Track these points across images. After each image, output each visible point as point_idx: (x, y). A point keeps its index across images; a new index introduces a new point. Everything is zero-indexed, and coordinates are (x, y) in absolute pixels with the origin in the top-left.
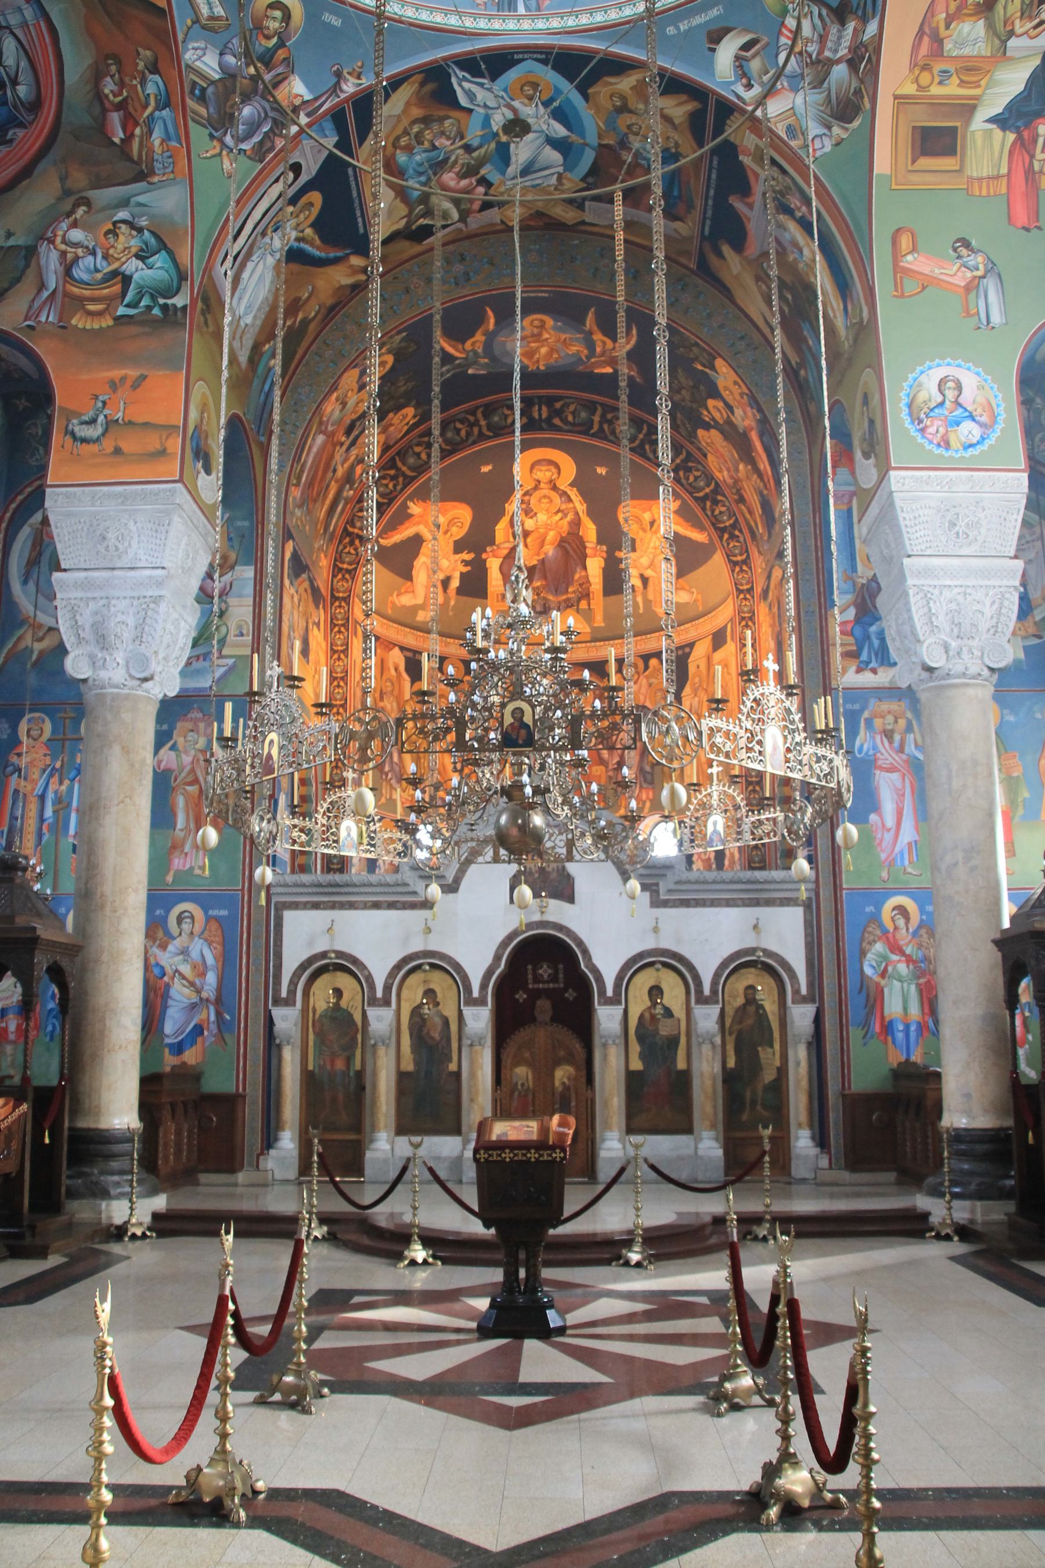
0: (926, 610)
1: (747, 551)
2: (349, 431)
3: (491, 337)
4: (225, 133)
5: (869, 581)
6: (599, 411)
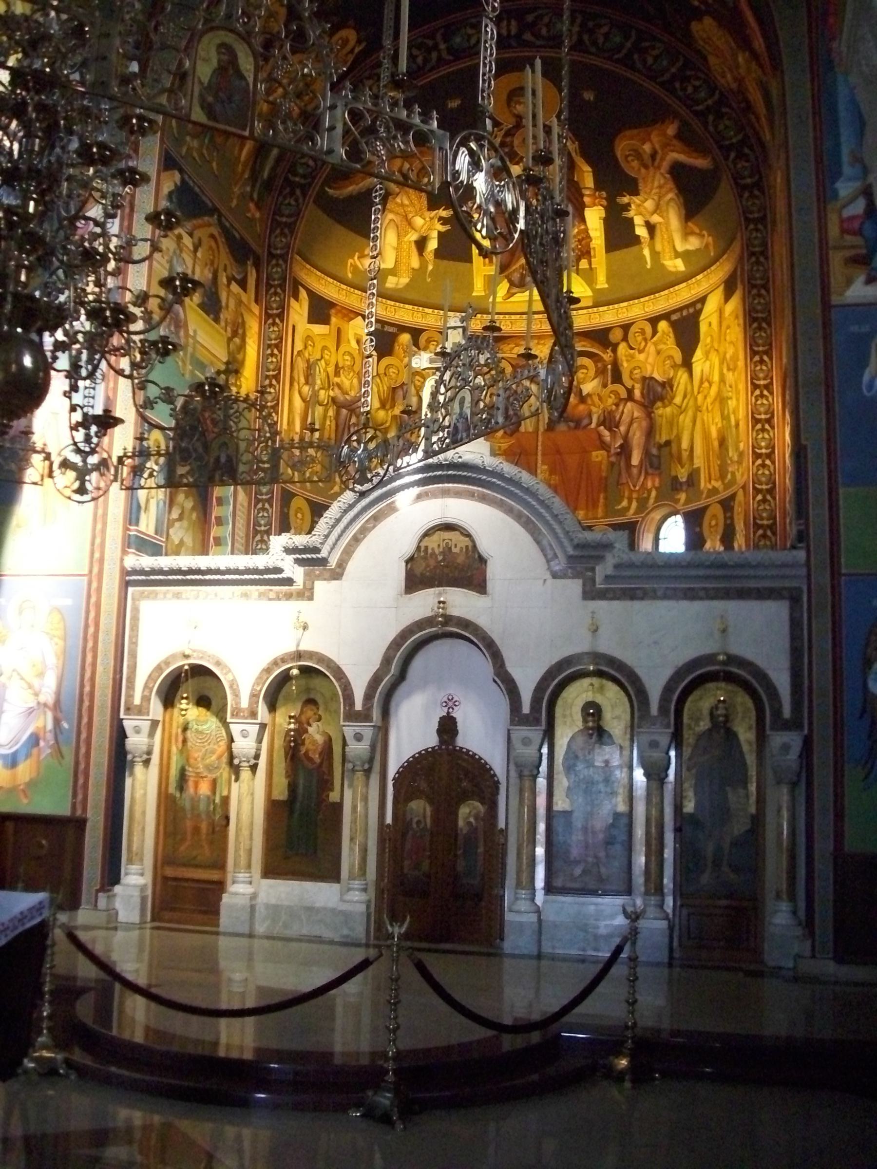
1: (759, 172)
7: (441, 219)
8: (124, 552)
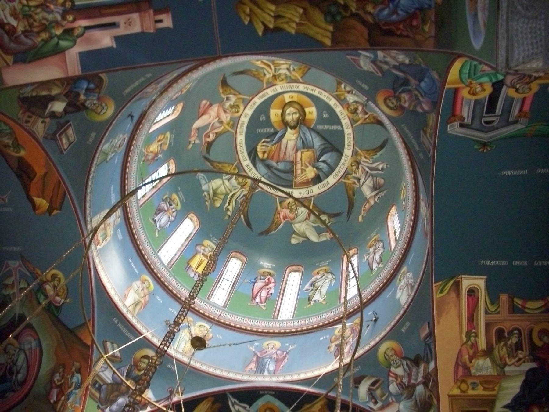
4: (107, 407)
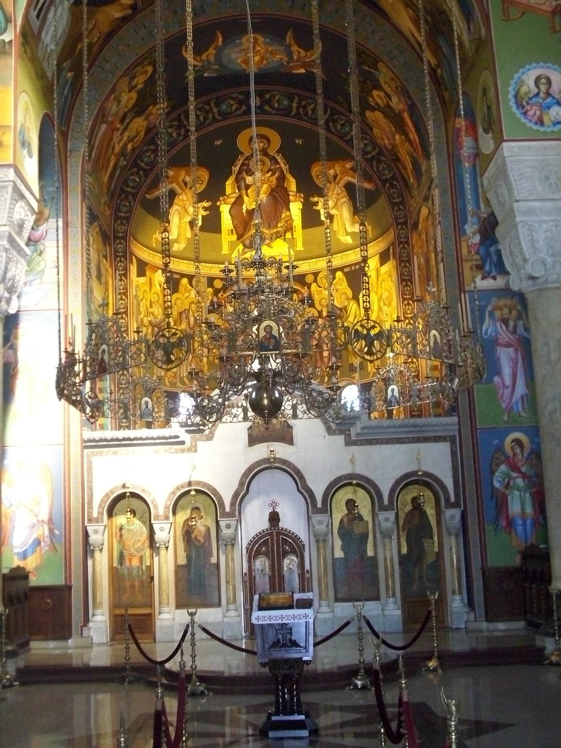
0: (530, 238)
1: (402, 195)
2: (122, 120)
3: (219, 50)
5: (489, 215)
6: (296, 100)
7: (204, 208)
8: (82, 430)
